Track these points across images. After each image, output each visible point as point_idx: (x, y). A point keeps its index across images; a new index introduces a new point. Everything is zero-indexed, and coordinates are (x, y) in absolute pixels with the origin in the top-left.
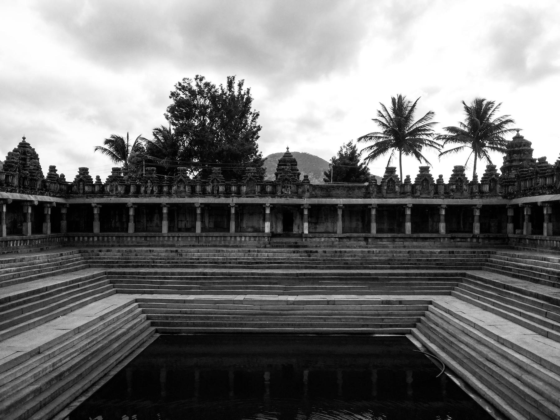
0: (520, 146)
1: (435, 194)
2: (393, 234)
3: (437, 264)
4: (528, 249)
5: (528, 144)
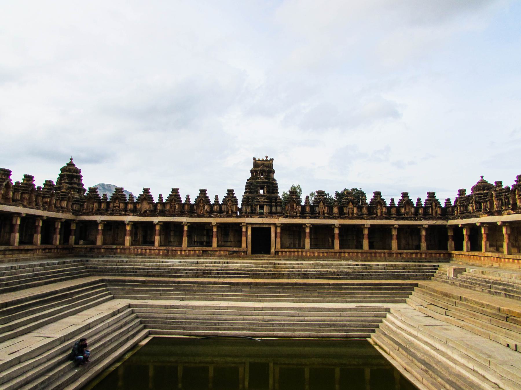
0: (77, 173)
1: (36, 205)
2: (7, 247)
3: (68, 275)
4: (109, 257)
5: (79, 171)
